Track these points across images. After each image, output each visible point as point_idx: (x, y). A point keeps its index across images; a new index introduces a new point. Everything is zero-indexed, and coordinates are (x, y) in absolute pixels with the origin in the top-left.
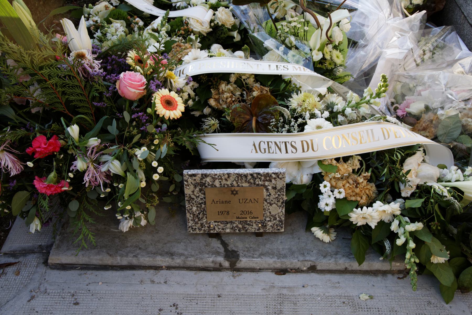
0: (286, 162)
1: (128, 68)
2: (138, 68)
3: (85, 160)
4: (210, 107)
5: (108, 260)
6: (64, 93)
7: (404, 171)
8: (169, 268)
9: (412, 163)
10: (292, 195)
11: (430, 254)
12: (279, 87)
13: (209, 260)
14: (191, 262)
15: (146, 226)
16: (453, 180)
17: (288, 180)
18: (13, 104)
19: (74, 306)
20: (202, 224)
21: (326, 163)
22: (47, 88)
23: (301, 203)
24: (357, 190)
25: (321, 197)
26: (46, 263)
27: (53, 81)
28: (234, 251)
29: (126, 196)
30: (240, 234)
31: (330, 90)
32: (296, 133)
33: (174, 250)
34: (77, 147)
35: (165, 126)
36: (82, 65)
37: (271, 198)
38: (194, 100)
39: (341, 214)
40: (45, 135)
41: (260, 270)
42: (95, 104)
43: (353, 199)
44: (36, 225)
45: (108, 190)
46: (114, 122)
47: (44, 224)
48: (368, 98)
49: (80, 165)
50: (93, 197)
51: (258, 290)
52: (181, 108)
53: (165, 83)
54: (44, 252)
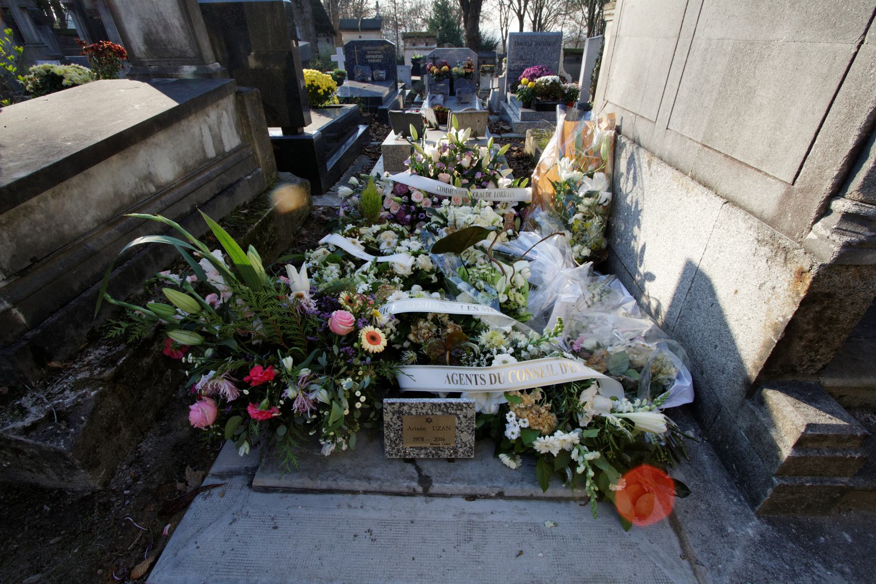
0: (475, 393)
1: (339, 307)
2: (348, 307)
3: (295, 389)
4: (410, 341)
5: (309, 484)
6: (282, 328)
7: (581, 403)
8: (366, 492)
9: (587, 395)
10: (482, 423)
11: (608, 482)
12: (470, 326)
13: (404, 485)
14: (386, 487)
15: (346, 450)
16: (625, 411)
17: (477, 409)
18: (237, 337)
19: (273, 531)
20: (398, 450)
21: (512, 395)
22: (268, 323)
23: (490, 431)
24: (540, 420)
25: (507, 425)
26: (250, 485)
27: (274, 318)
28: (427, 477)
29: (330, 422)
30: (433, 459)
31: (515, 328)
32: (484, 366)
33: (372, 474)
34: (289, 376)
35: (368, 359)
36: (300, 304)
37: (462, 426)
38: (395, 335)
39: (526, 443)
40: (262, 365)
41: (451, 496)
42: (309, 338)
43: (536, 428)
44: (245, 449)
45: (314, 416)
46: (324, 354)
47: (252, 447)
48: (547, 336)
49: (290, 392)
50: (300, 422)
51: (449, 516)
52: (384, 342)
53: (371, 321)
54: (250, 474)
